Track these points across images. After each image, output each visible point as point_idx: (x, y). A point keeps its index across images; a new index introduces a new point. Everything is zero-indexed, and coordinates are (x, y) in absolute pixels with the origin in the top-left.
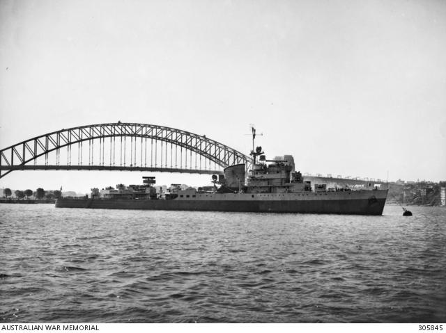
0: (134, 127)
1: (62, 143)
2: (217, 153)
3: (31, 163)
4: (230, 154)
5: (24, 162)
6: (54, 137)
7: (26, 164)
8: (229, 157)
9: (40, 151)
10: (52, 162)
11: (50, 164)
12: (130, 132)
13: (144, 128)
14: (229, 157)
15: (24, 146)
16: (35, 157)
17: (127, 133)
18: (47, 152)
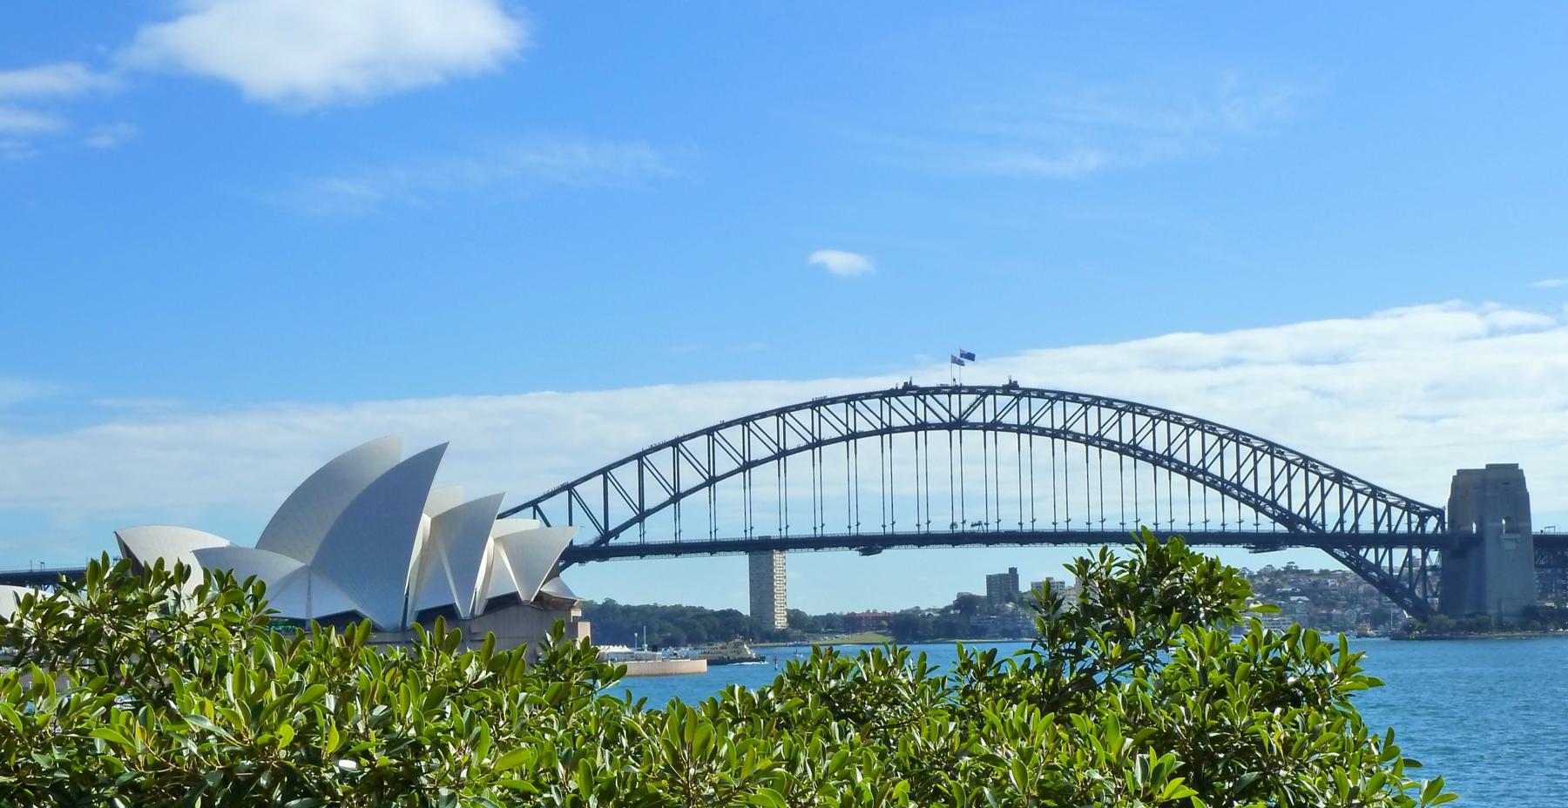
0: (955, 397)
1: (724, 464)
2: (1281, 484)
3: (630, 537)
4: (1328, 483)
5: (607, 535)
6: (698, 446)
7: (612, 541)
8: (1324, 496)
9: (656, 495)
10: (695, 532)
11: (688, 536)
12: (946, 418)
13: (990, 398)
14: (1324, 496)
15: (606, 478)
16: (642, 515)
17: (932, 419)
18: (676, 498)
